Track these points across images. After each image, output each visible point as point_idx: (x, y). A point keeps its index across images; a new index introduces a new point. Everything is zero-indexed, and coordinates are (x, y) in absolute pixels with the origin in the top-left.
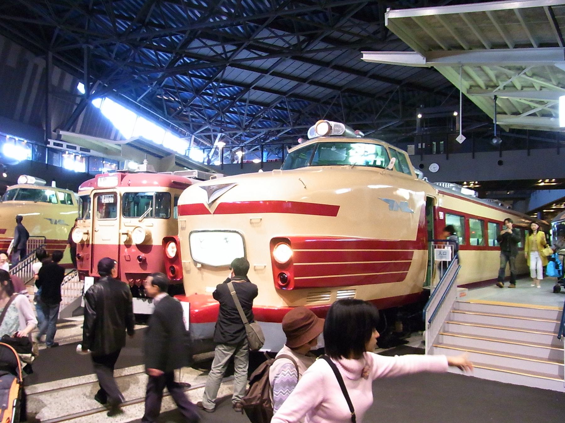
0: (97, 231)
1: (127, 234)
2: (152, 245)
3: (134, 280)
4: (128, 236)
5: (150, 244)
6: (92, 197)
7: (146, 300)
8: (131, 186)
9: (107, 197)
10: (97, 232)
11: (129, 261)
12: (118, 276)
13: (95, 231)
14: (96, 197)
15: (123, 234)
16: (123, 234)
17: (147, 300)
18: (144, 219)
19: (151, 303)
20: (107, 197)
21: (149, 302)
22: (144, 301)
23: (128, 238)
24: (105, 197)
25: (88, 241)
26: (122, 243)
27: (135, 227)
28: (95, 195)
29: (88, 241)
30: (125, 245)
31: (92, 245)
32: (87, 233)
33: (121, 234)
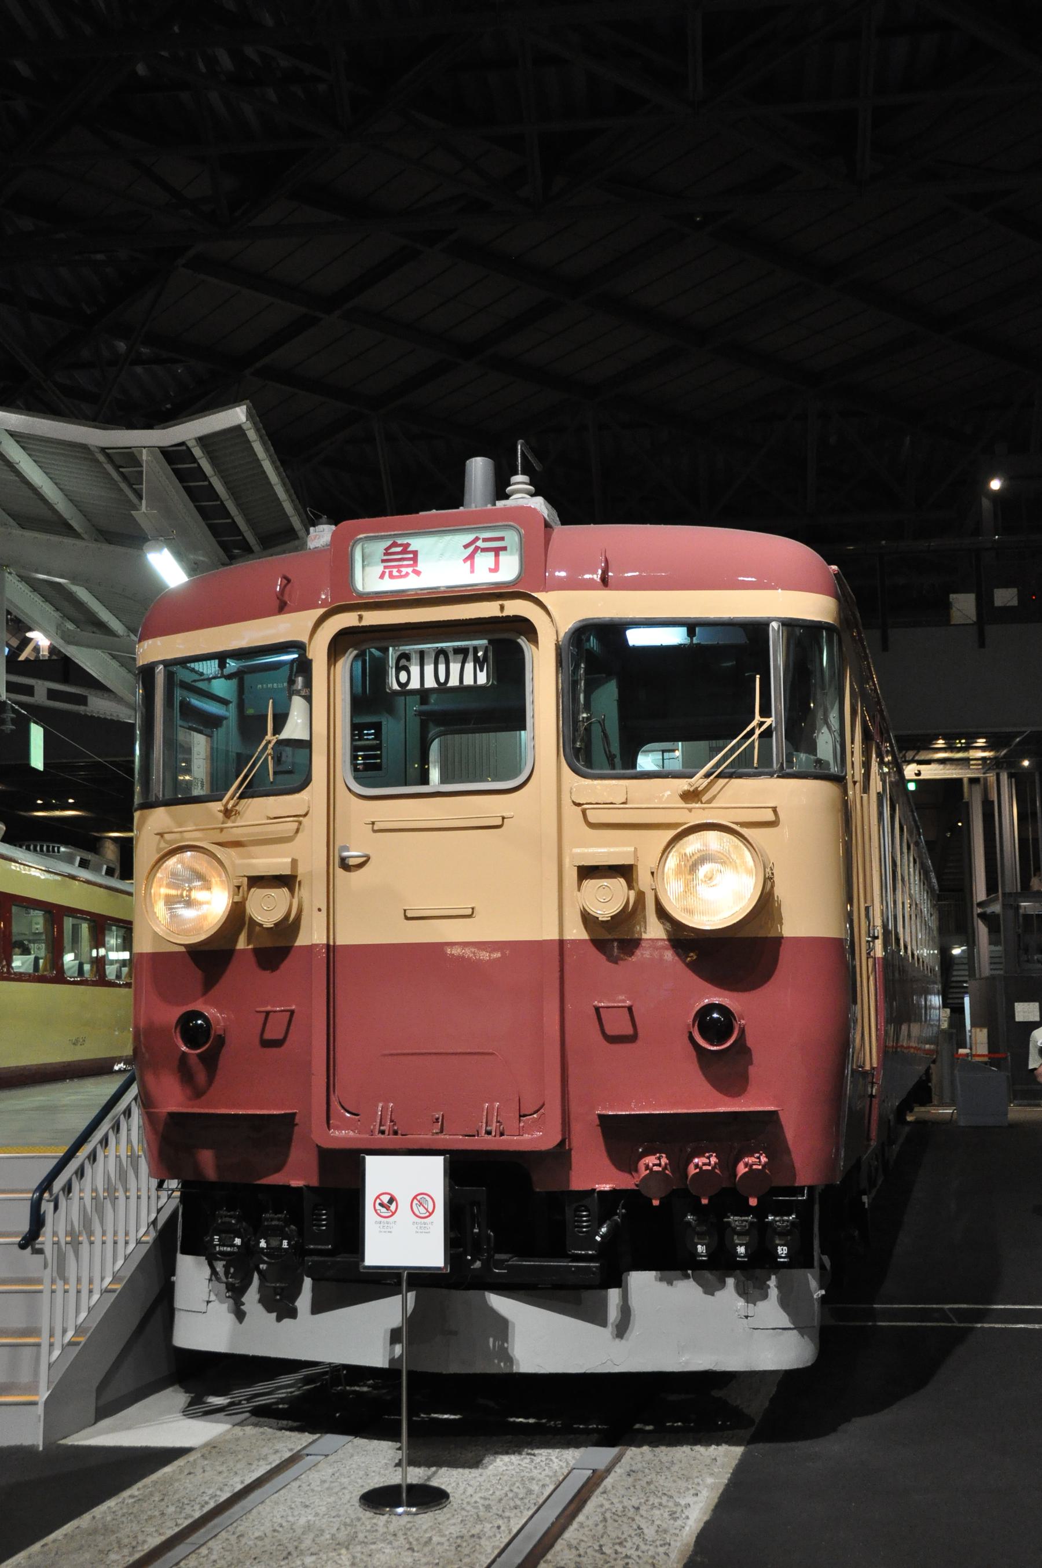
0: (360, 866)
1: (625, 872)
2: (779, 940)
3: (680, 1164)
4: (630, 886)
5: (761, 934)
6: (318, 653)
7: (723, 1284)
8: (611, 590)
9: (422, 654)
10: (355, 875)
11: (632, 1038)
12: (562, 1143)
13: (345, 865)
14: (344, 653)
15: (587, 872)
16: (587, 872)
17: (730, 1282)
18: (722, 782)
19: (765, 1296)
20: (422, 654)
21: (742, 1291)
22: (709, 1290)
23: (632, 894)
24: (406, 656)
25: (289, 927)
26: (576, 932)
27: (671, 834)
28: (339, 645)
29: (289, 927)
30: (600, 944)
31: (330, 949)
32: (286, 881)
33: (572, 875)
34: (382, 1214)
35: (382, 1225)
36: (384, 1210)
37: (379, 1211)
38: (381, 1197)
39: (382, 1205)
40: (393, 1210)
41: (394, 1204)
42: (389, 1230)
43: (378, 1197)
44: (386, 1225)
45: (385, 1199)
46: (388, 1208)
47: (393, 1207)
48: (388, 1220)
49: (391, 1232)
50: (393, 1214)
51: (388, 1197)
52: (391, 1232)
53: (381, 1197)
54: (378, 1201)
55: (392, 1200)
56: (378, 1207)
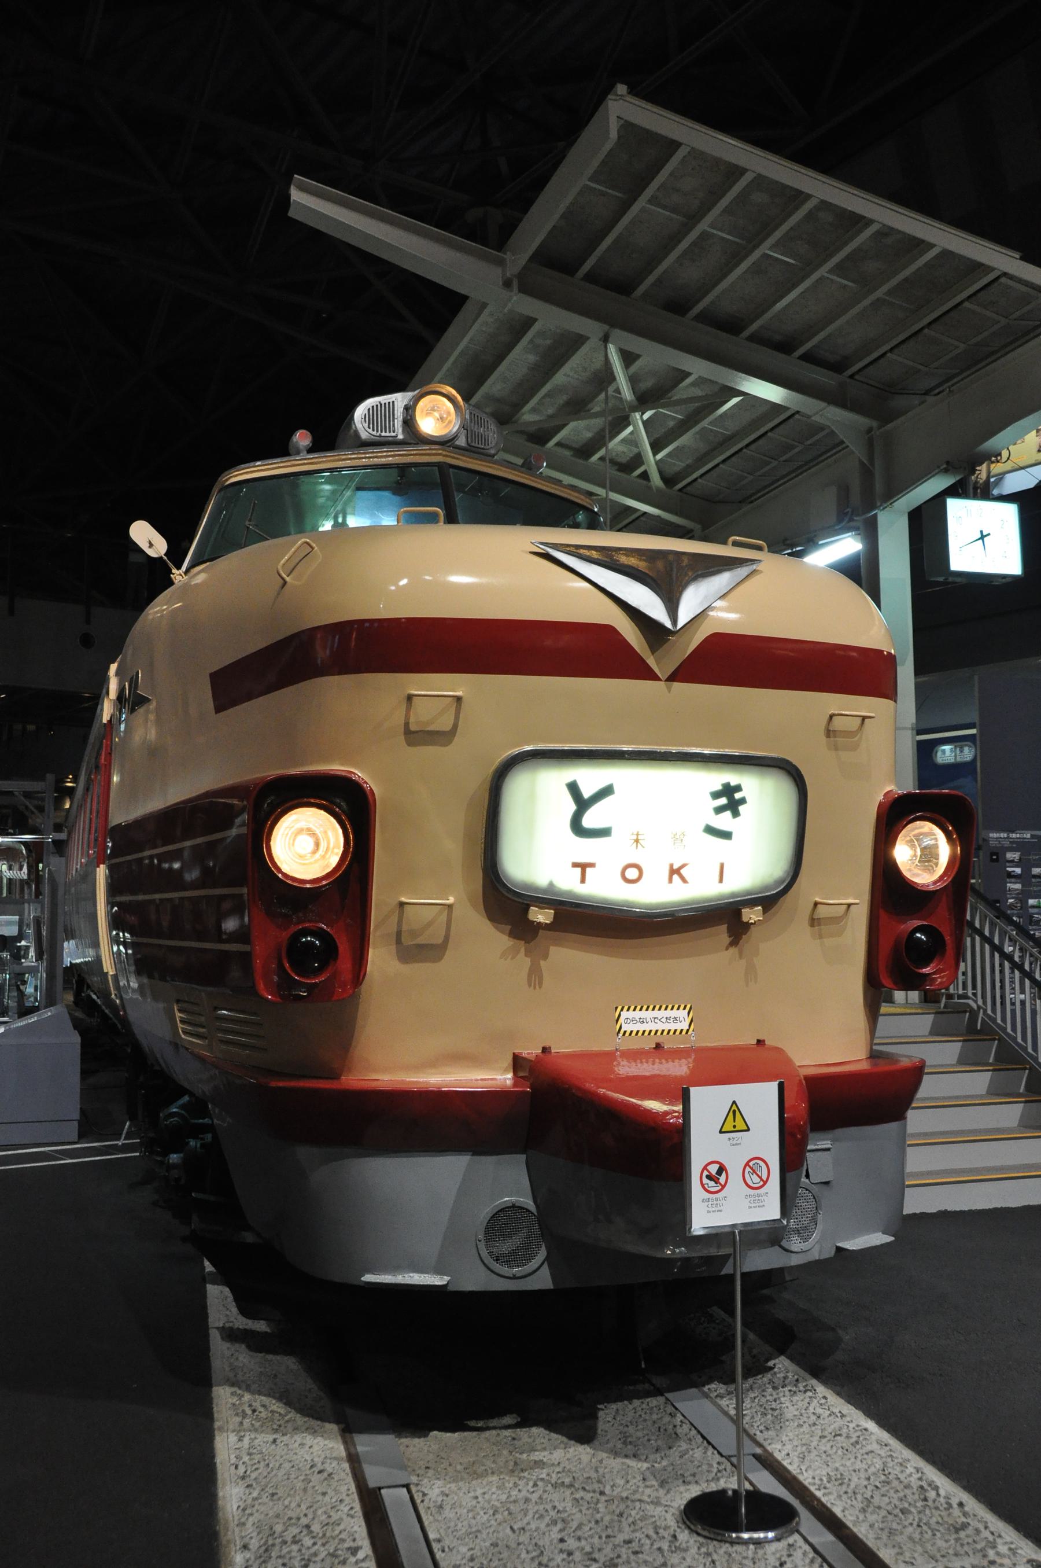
34: (710, 1189)
35: (710, 1203)
36: (712, 1183)
37: (706, 1186)
38: (709, 1168)
39: (710, 1177)
40: (723, 1183)
41: (724, 1173)
42: (720, 1208)
43: (705, 1168)
44: (715, 1202)
45: (713, 1169)
46: (717, 1181)
47: (722, 1179)
48: (714, 1196)
49: (721, 1211)
50: (723, 1187)
51: (717, 1166)
52: (721, 1211)
53: (708, 1168)
54: (706, 1173)
55: (722, 1169)
56: (705, 1181)
